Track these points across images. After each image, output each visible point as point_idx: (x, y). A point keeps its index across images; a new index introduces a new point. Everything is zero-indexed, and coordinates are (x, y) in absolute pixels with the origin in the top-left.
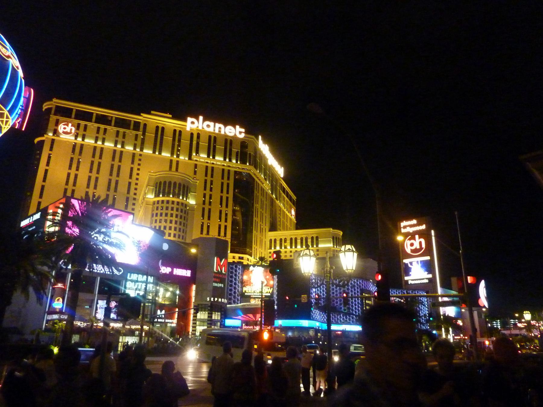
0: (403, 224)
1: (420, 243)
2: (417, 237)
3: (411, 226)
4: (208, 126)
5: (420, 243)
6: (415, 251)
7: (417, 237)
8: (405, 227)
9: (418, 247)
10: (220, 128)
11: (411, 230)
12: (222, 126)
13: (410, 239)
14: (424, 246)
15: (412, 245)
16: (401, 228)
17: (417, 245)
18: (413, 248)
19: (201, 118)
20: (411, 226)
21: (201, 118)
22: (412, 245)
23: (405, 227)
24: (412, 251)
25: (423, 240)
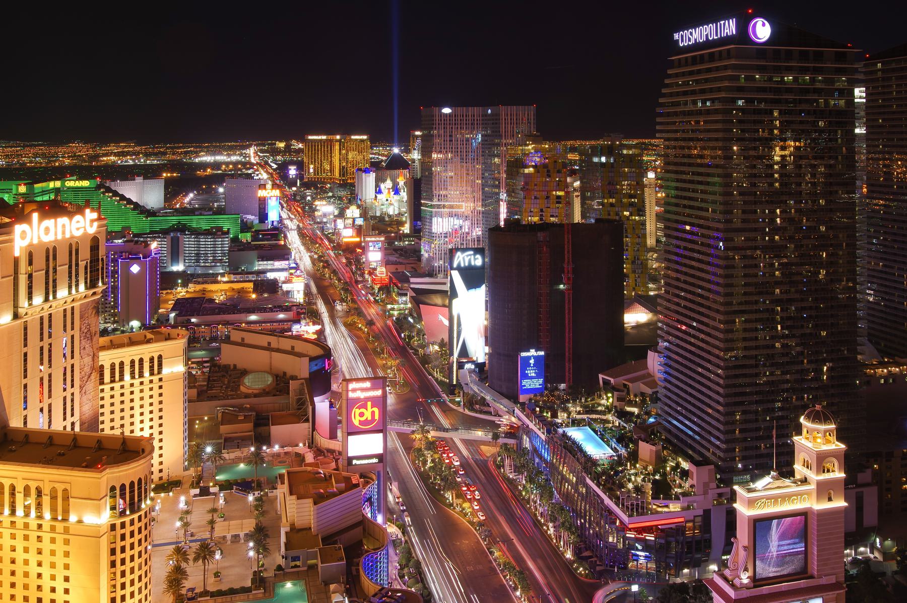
0: (352, 386)
1: (373, 413)
2: (369, 404)
3: (363, 390)
4: (47, 230)
5: (373, 413)
6: (365, 423)
7: (369, 404)
8: (354, 390)
9: (370, 418)
10: (64, 226)
11: (362, 395)
12: (63, 220)
13: (359, 408)
14: (377, 417)
15: (362, 415)
16: (347, 391)
17: (368, 415)
18: (363, 419)
19: (35, 216)
20: (363, 390)
21: (35, 216)
22: (362, 415)
23: (354, 390)
24: (361, 422)
25: (376, 410)
